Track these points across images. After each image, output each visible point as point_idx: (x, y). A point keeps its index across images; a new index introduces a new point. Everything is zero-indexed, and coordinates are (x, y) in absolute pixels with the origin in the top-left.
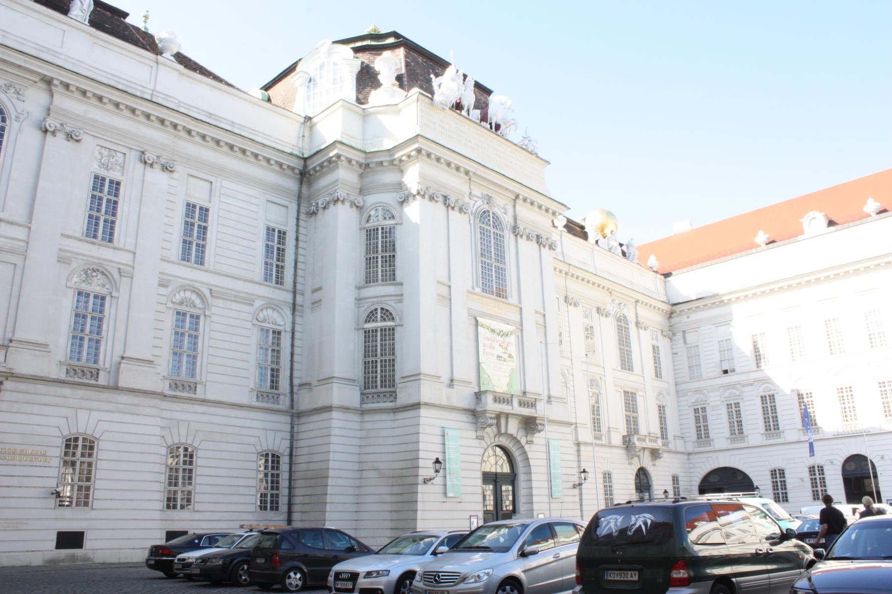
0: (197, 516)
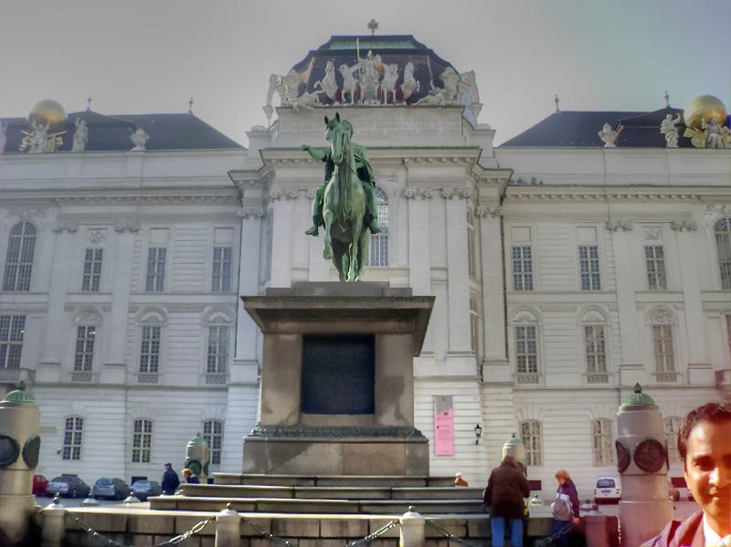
0: (154, 467)
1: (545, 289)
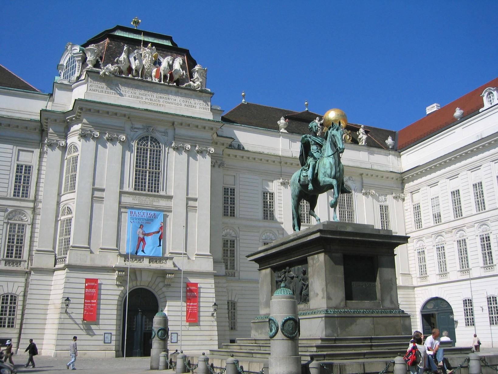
1: (240, 216)
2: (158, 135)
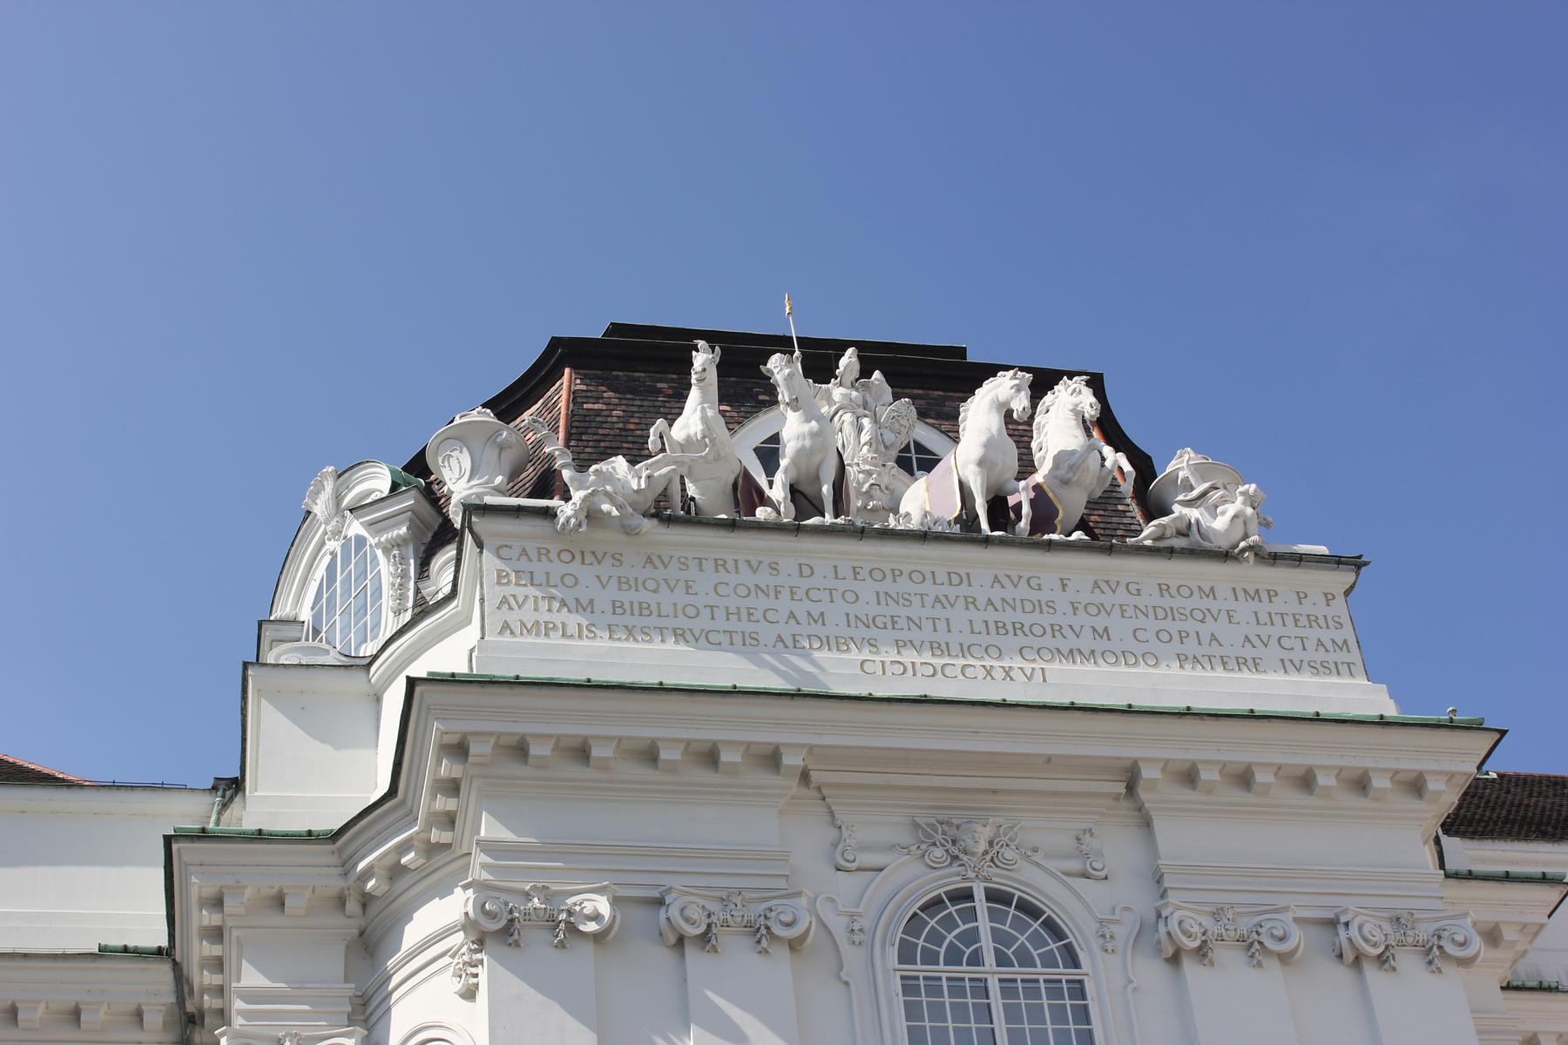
2: (1033, 880)
